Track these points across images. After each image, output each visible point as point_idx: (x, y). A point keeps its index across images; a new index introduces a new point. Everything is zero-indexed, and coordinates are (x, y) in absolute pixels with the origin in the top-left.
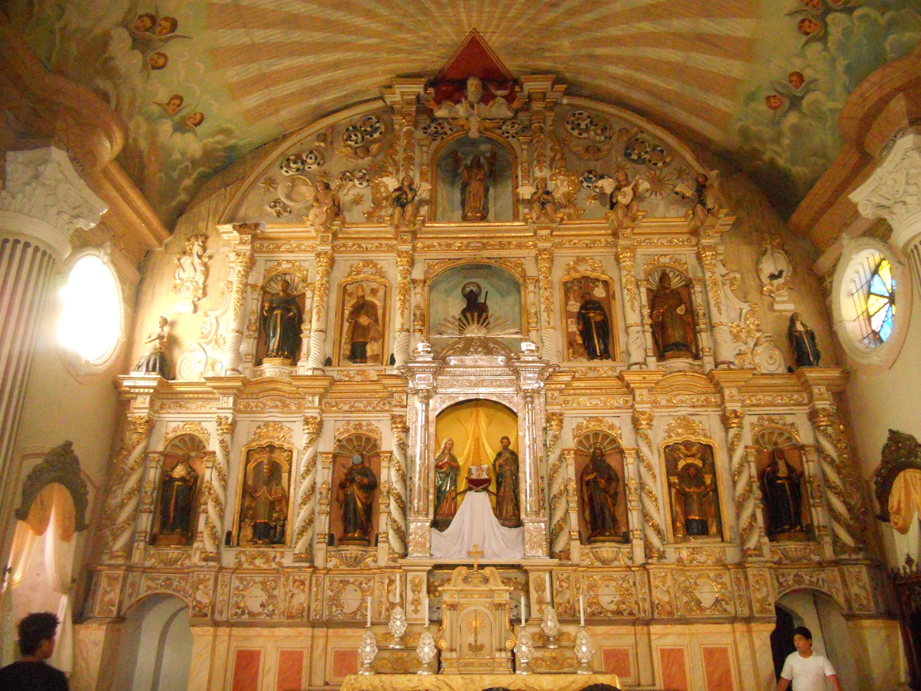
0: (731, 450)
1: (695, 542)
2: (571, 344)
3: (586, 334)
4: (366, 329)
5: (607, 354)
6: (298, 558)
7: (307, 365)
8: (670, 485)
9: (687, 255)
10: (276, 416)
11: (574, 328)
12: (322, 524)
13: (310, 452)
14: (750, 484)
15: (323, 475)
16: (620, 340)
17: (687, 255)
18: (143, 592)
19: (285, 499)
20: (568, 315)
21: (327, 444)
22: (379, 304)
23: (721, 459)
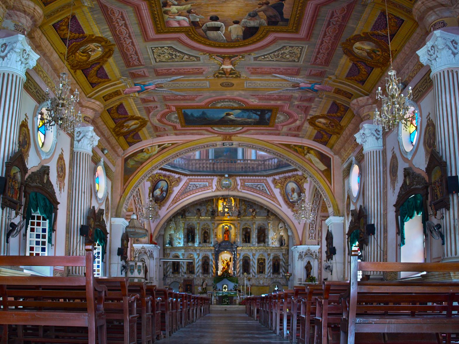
0: (268, 260)
1: (261, 274)
2: (243, 240)
3: (246, 238)
4: (206, 237)
5: (249, 242)
6: (197, 276)
7: (196, 245)
8: (258, 265)
9: (266, 223)
10: (191, 252)
11: (244, 237)
12: (201, 271)
13: (198, 260)
14: (270, 265)
15: (200, 263)
16: (252, 240)
17: (266, 223)
18: (172, 281)
19: (194, 267)
20: (243, 234)
21: (200, 258)
22: (209, 232)
23: (266, 261)
